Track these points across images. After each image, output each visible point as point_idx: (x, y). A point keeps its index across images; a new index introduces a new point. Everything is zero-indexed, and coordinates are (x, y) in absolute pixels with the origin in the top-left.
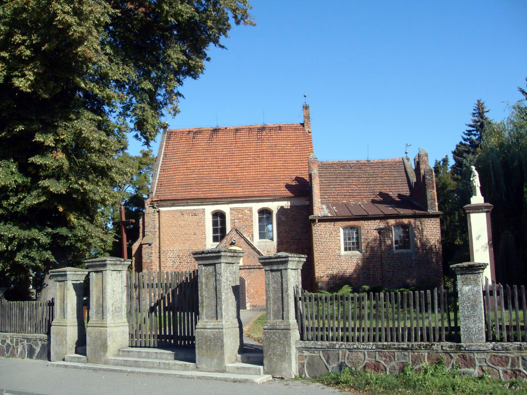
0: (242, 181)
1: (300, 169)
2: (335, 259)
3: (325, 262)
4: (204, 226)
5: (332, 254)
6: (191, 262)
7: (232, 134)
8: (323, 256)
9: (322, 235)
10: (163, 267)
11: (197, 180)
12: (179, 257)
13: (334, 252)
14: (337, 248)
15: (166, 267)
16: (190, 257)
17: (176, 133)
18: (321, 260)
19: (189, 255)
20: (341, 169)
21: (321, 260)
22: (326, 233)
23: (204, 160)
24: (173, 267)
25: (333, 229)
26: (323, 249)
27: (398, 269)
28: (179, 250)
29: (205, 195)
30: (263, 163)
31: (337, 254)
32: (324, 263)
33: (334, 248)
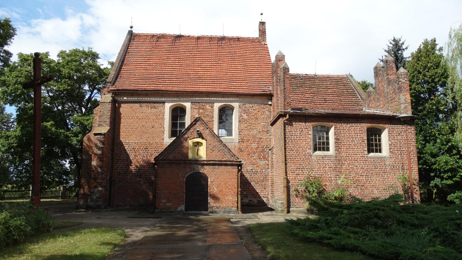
0: (204, 78)
1: (260, 73)
2: (306, 159)
3: (295, 162)
4: (163, 119)
5: (303, 153)
6: (147, 156)
7: (193, 41)
8: (293, 155)
9: (292, 131)
10: (116, 159)
11: (158, 75)
12: (134, 151)
13: (304, 151)
14: (307, 147)
15: (120, 160)
16: (146, 151)
17: (139, 36)
18: (290, 158)
19: (145, 149)
20: (293, 80)
21: (290, 158)
22: (297, 130)
23: (166, 59)
24: (127, 160)
25: (304, 127)
26: (293, 147)
27: (372, 174)
28: (135, 143)
29: (166, 88)
30: (224, 65)
31: (308, 153)
32: (294, 163)
33: (304, 147)
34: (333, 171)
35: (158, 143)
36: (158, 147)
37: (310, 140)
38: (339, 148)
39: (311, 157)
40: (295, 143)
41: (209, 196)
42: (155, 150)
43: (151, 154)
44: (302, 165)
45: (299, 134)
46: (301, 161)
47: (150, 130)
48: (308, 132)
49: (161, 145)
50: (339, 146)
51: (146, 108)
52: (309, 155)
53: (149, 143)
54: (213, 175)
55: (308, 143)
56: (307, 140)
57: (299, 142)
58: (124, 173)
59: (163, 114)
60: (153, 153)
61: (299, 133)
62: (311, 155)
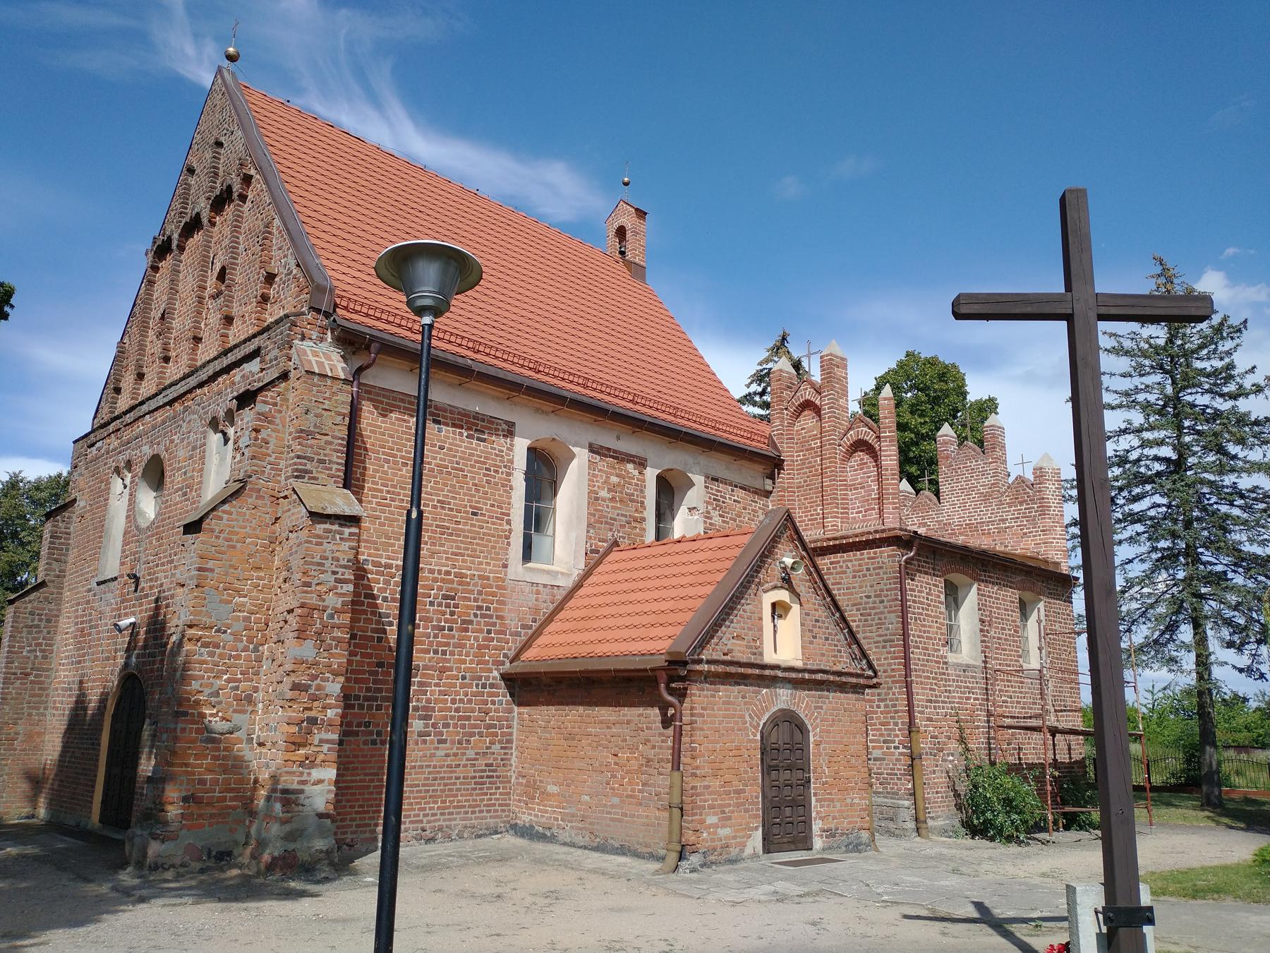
6: (451, 629)
16: (448, 606)
19: (445, 597)
24: (380, 640)
35: (488, 578)
36: (487, 594)
39: (947, 669)
41: (815, 794)
42: (479, 608)
43: (464, 622)
47: (465, 524)
49: (497, 587)
51: (454, 433)
53: (461, 576)
54: (818, 721)
58: (367, 699)
59: (509, 465)
60: (472, 617)
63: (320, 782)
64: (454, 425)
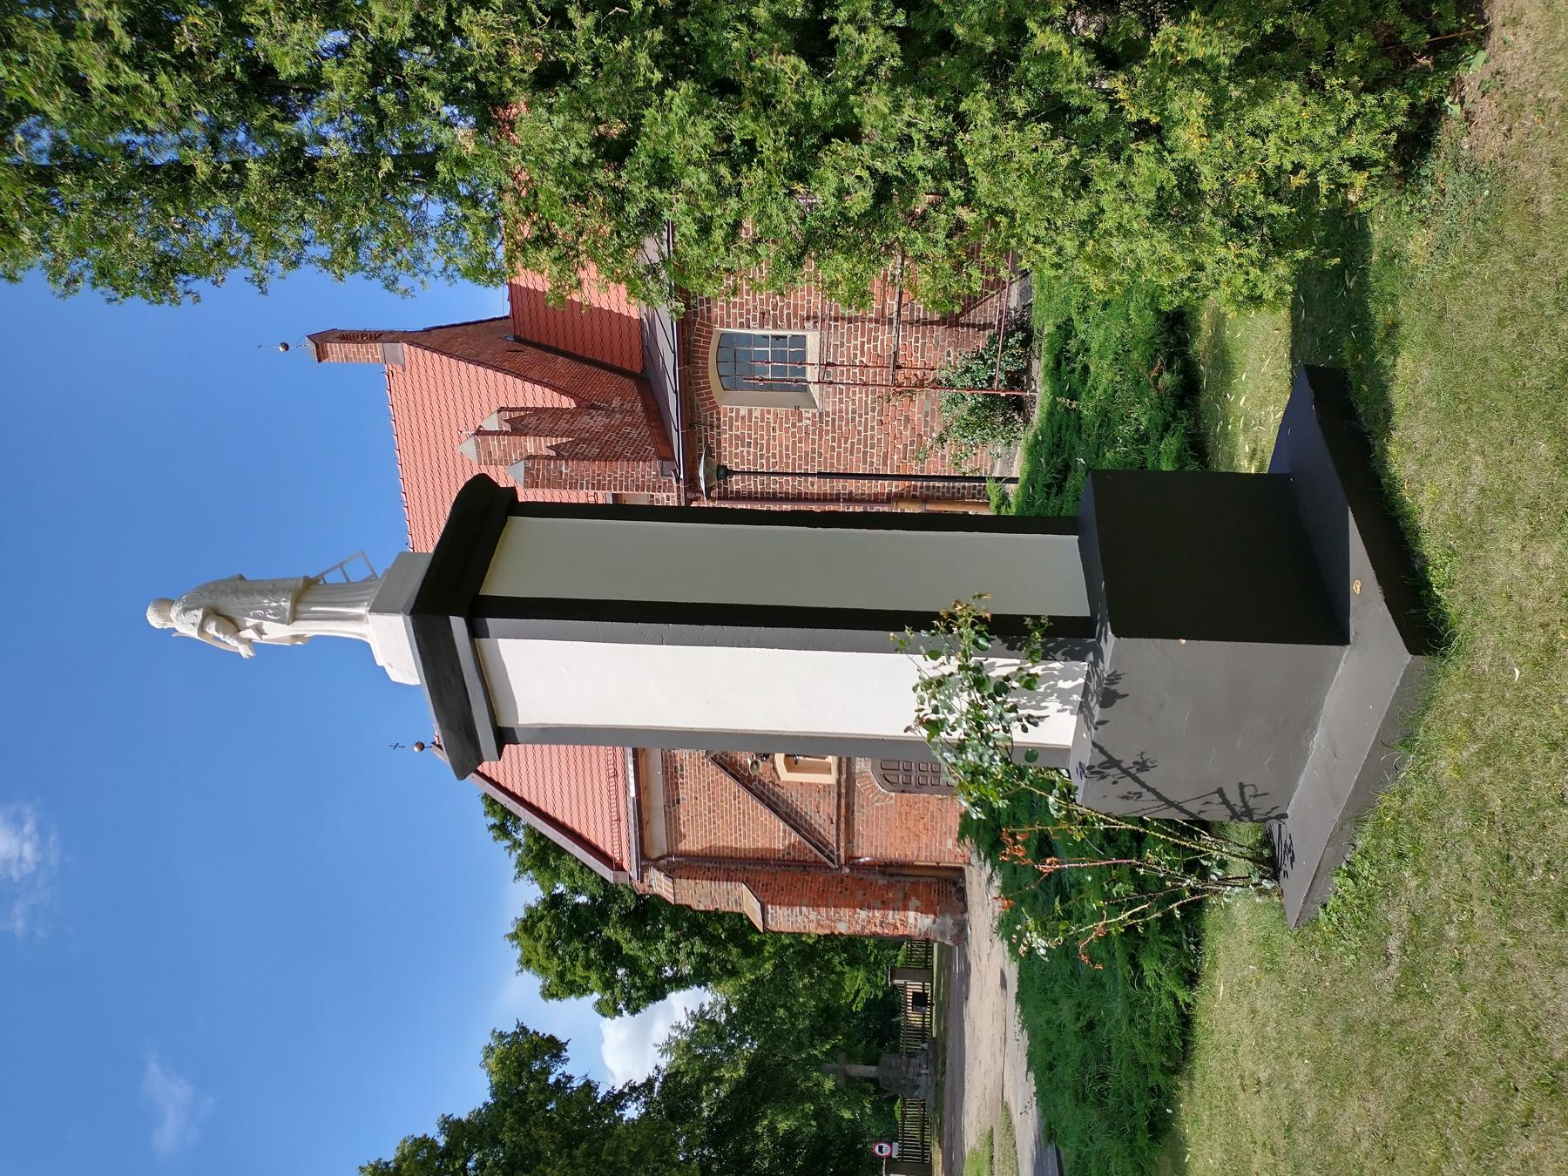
2: (834, 432)
22: (736, 454)
31: (814, 424)
34: (876, 340)
37: (769, 412)
38: (795, 317)
39: (827, 414)
40: (781, 462)
44: (853, 443)
45: (752, 450)
46: (840, 447)
48: (743, 418)
50: (788, 314)
52: (821, 422)
55: (781, 423)
56: (768, 423)
57: (777, 452)
61: (745, 449)
62: (821, 414)
63: (916, 919)
64: (677, 789)
